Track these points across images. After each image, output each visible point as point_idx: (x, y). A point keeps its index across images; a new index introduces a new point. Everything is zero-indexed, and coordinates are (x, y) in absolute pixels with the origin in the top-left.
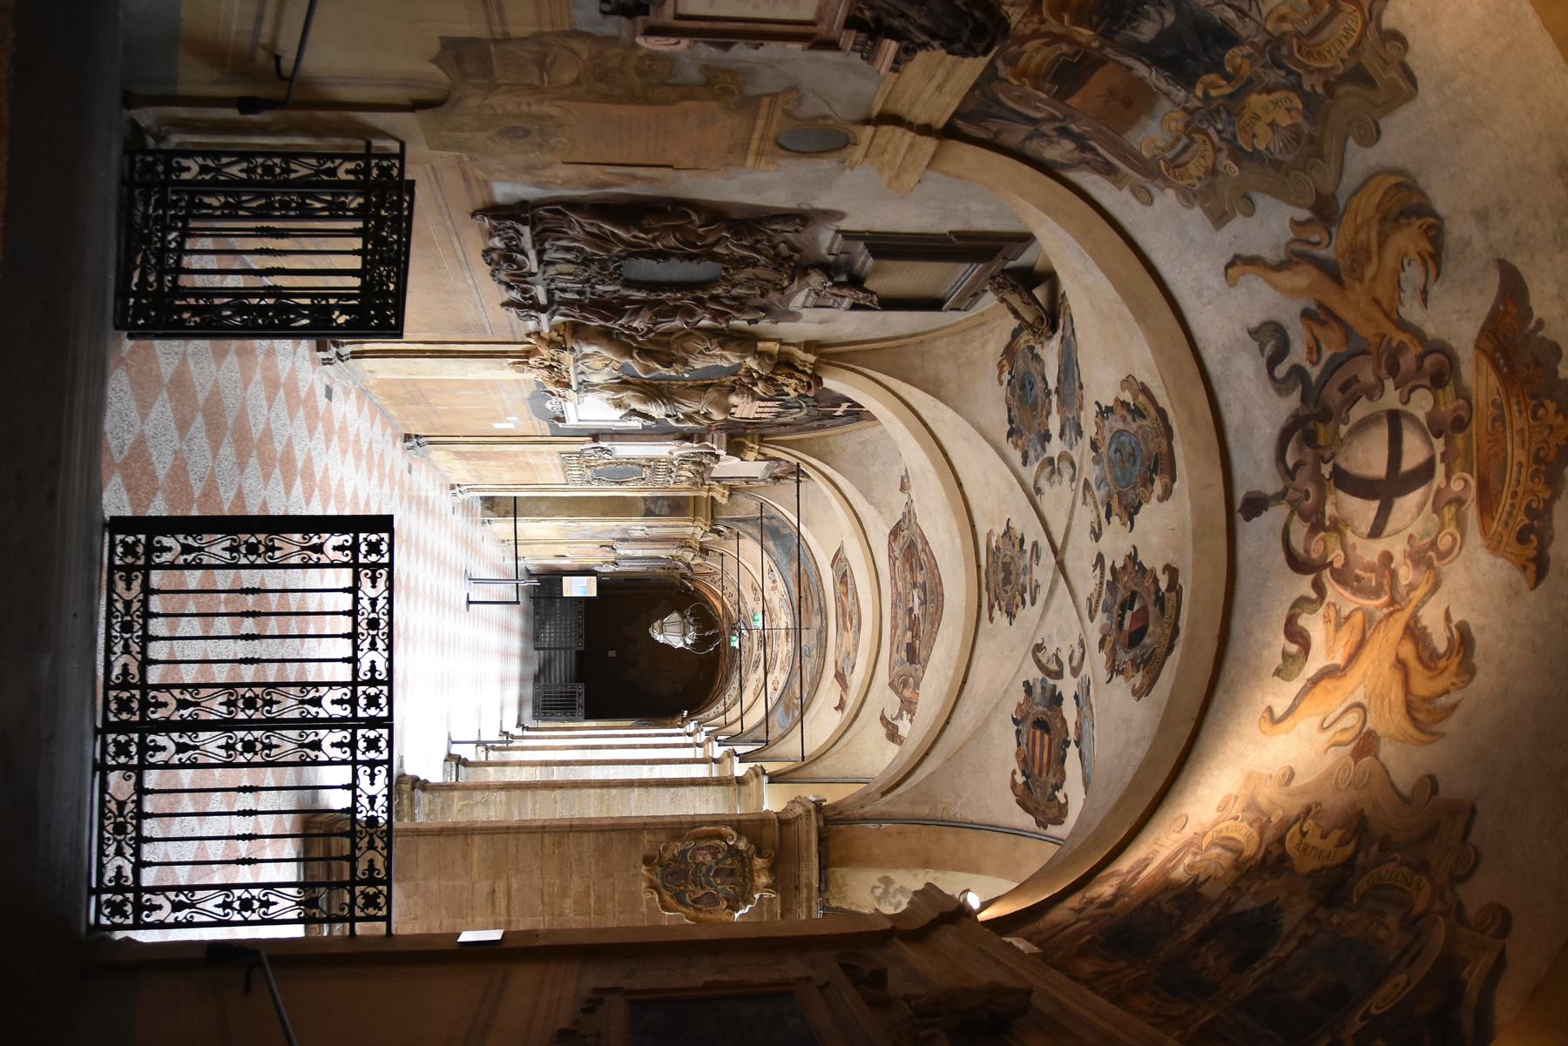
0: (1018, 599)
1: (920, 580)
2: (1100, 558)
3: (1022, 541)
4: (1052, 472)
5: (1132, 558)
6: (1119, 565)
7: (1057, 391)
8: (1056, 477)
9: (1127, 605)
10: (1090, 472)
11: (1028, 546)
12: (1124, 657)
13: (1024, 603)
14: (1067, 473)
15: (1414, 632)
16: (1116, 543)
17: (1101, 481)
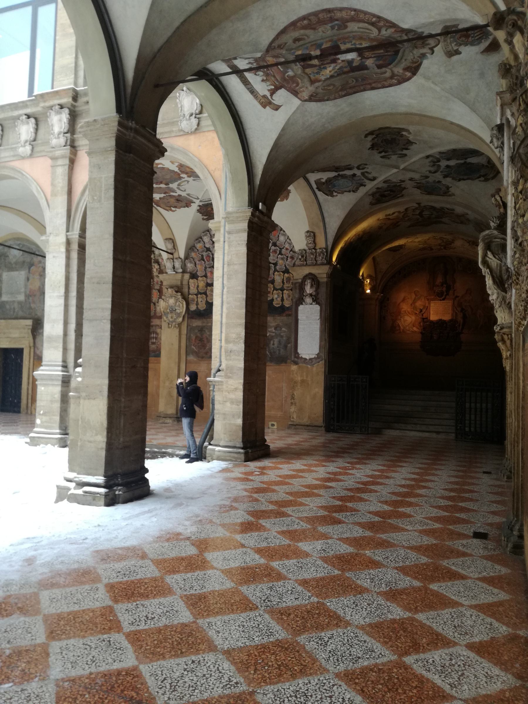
0: (381, 150)
1: (369, 62)
2: (404, 181)
3: (407, 149)
4: (434, 162)
5: (405, 188)
6: (403, 186)
7: (465, 162)
8: (432, 164)
9: (391, 191)
10: (431, 180)
11: (405, 152)
12: (377, 195)
13: (380, 153)
14: (432, 169)
15: (398, 222)
16: (408, 184)
17: (428, 182)
